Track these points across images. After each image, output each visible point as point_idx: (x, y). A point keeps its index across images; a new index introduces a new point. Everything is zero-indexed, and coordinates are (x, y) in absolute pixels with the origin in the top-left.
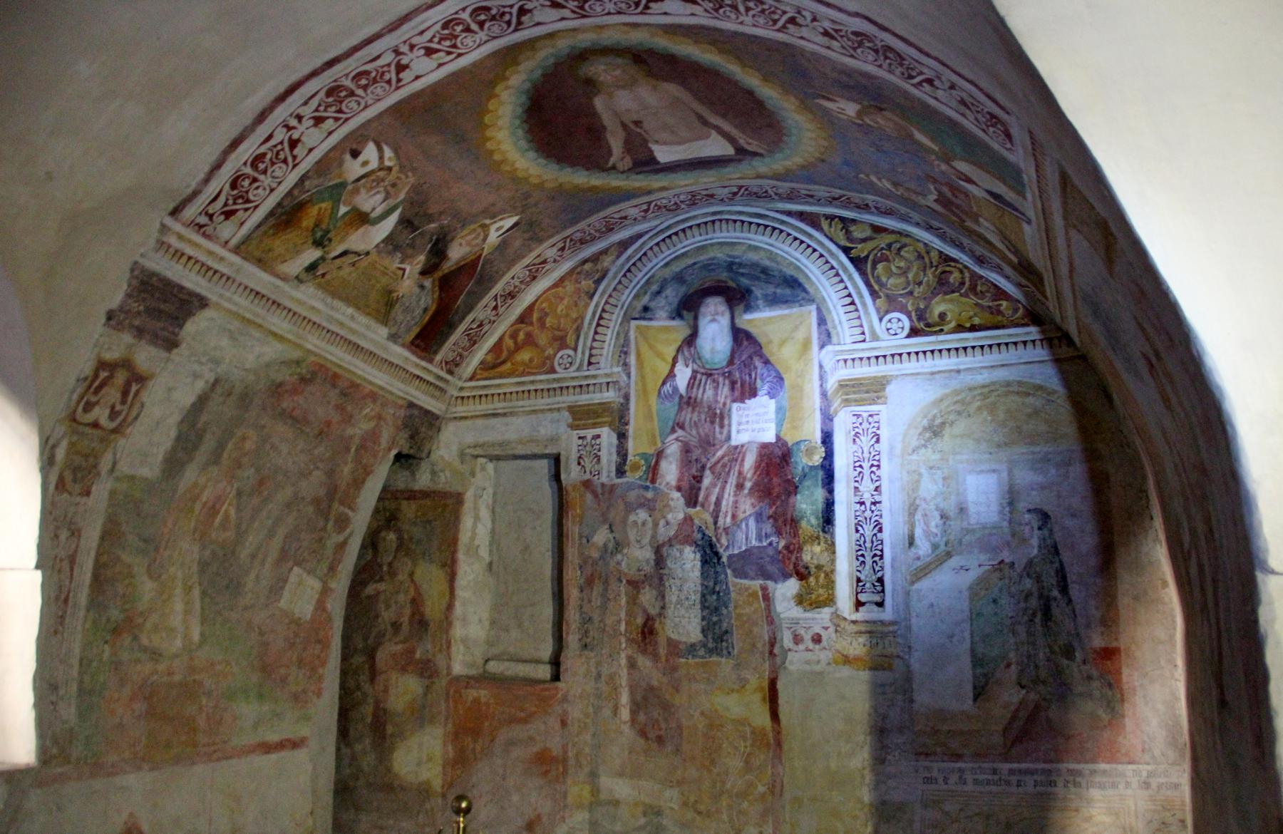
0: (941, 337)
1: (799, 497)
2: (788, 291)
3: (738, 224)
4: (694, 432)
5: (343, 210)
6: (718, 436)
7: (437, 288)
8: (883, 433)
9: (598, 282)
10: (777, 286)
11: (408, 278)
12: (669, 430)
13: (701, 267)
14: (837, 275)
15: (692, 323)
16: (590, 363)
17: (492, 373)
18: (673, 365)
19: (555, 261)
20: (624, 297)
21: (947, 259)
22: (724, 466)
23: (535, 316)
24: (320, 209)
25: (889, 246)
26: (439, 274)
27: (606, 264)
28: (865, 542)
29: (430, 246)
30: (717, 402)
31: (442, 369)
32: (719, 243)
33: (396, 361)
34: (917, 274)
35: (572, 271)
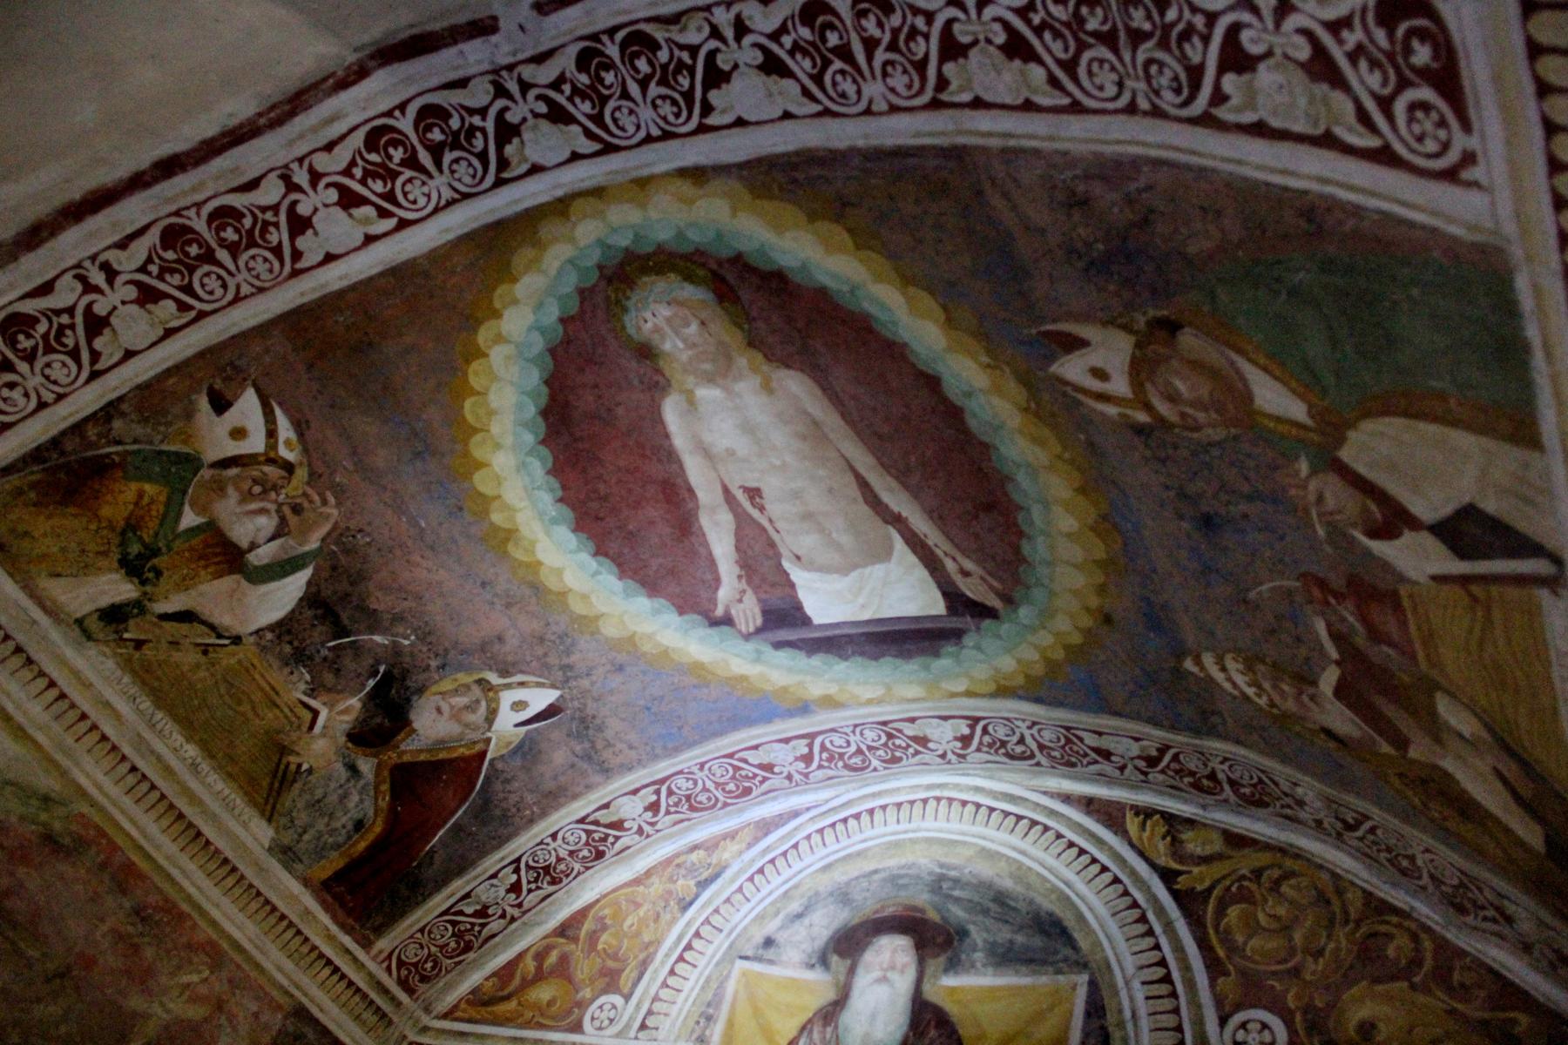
3: (970, 808)
5: (189, 519)
7: (385, 787)
9: (703, 885)
11: (323, 735)
13: (884, 880)
14: (1143, 919)
15: (842, 978)
16: (643, 1027)
17: (483, 1010)
19: (640, 831)
21: (1378, 908)
23: (588, 926)
24: (141, 494)
25: (1258, 873)
26: (392, 757)
27: (726, 855)
29: (371, 683)
31: (389, 969)
33: (282, 907)
35: (668, 862)
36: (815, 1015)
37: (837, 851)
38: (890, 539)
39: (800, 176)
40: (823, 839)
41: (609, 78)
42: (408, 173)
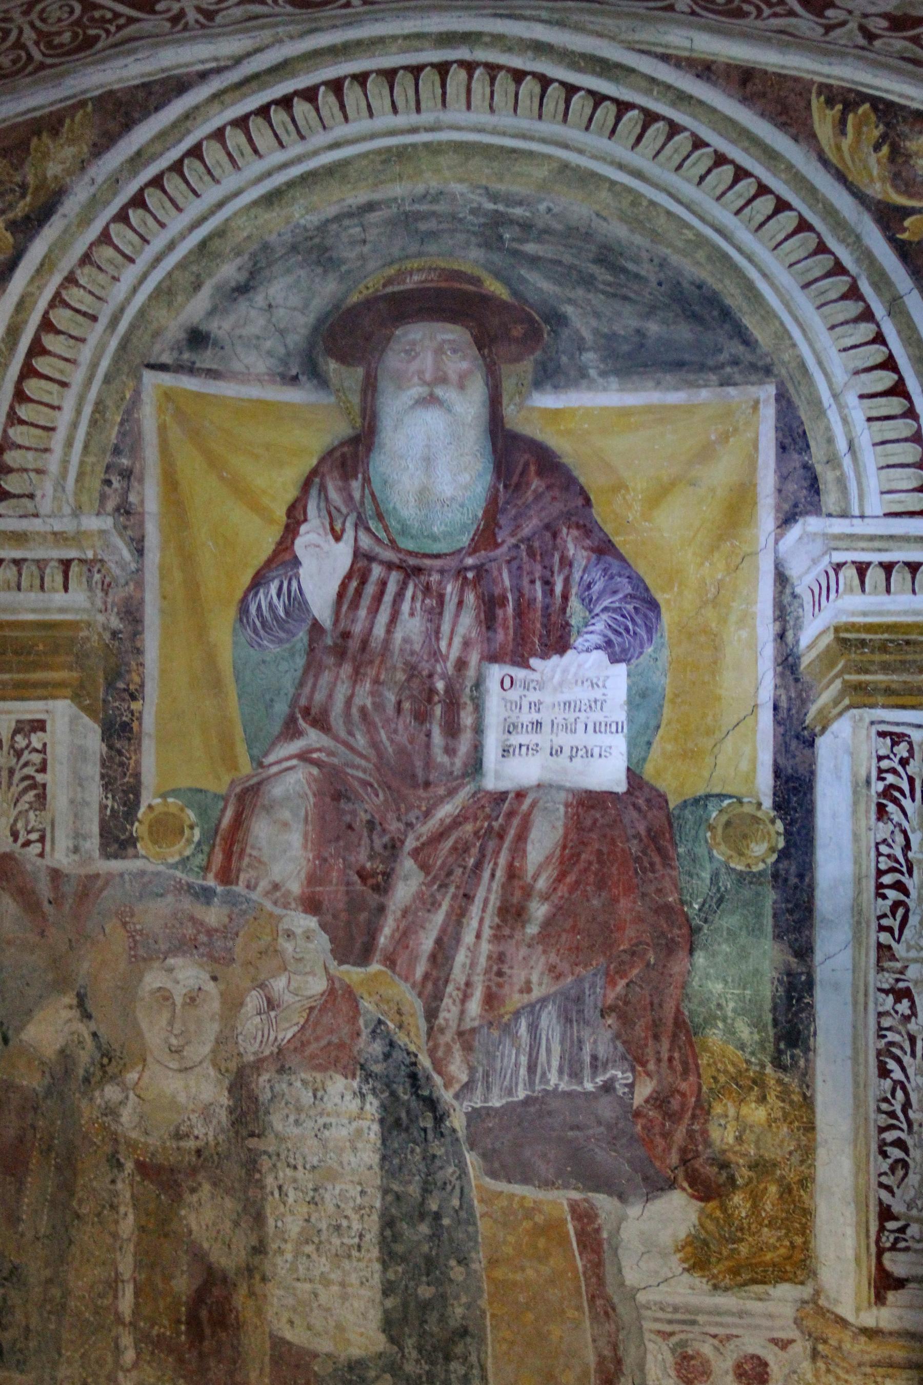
1: (700, 959)
2: (684, 332)
3: (529, 86)
4: (361, 741)
6: (440, 757)
10: (651, 311)
12: (277, 727)
13: (392, 222)
15: (355, 399)
18: (291, 529)
20: (120, 290)
22: (461, 850)
28: (907, 1105)
30: (436, 655)
32: (458, 147)
36: (322, 460)
37: (284, 166)
40: (250, 140)
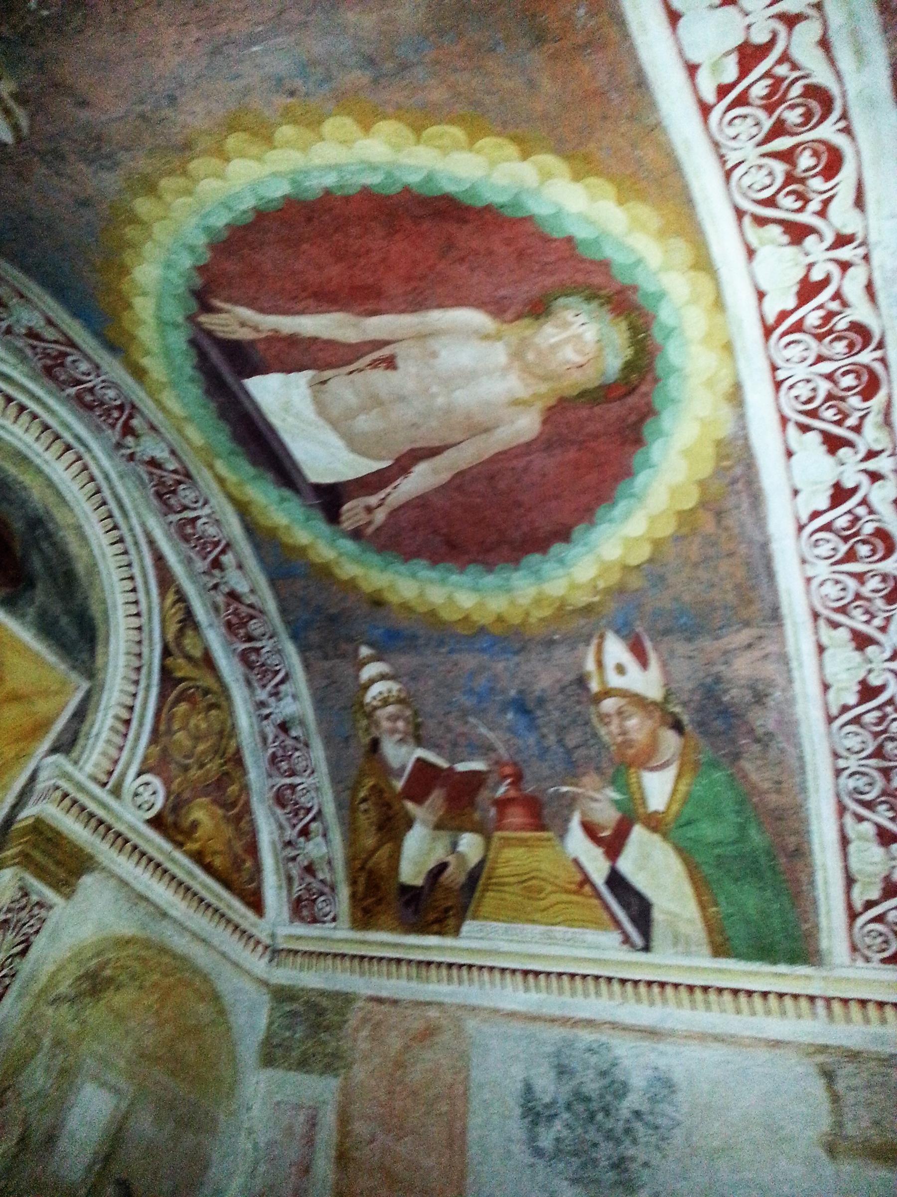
0: (178, 855)
2: (73, 633)
8: (39, 943)
10: (68, 612)
21: (238, 760)
25: (207, 692)
34: (203, 753)
38: (381, 458)
39: (739, 486)
41: (840, 347)
42: (768, 124)
